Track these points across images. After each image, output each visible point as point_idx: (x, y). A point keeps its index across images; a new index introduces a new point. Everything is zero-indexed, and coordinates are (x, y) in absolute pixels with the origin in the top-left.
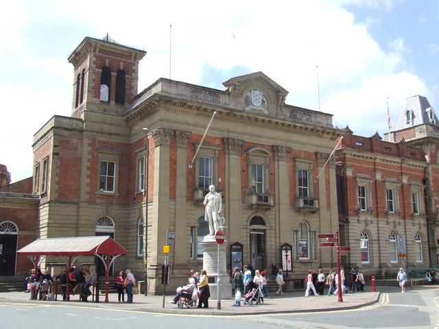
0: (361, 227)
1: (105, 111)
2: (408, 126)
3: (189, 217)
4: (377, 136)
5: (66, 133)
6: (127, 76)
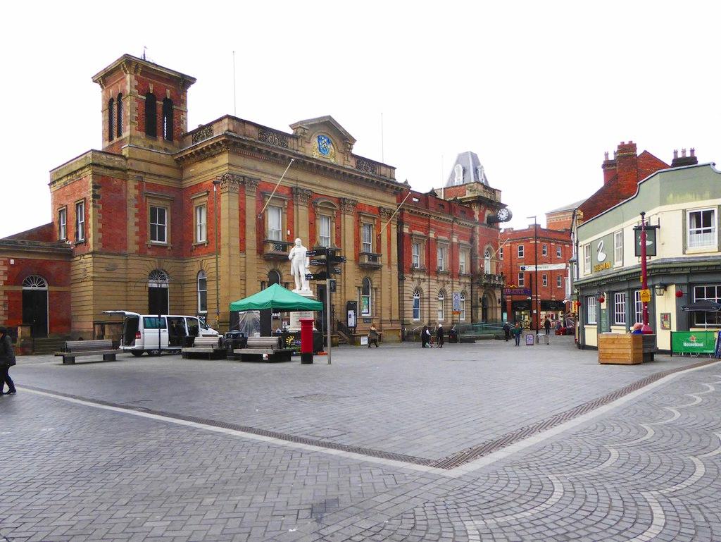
0: (415, 284)
5: (107, 172)
6: (174, 107)
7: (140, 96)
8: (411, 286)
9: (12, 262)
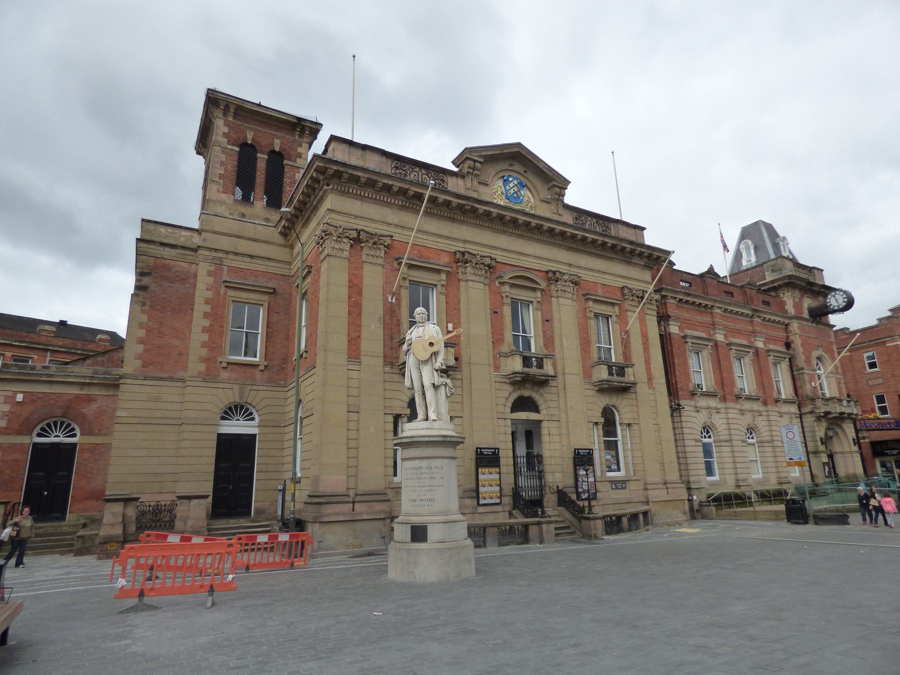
1: (243, 215)
3: (389, 394)
4: (711, 272)
6: (285, 162)
7: (230, 147)
8: (695, 420)
9: (20, 397)
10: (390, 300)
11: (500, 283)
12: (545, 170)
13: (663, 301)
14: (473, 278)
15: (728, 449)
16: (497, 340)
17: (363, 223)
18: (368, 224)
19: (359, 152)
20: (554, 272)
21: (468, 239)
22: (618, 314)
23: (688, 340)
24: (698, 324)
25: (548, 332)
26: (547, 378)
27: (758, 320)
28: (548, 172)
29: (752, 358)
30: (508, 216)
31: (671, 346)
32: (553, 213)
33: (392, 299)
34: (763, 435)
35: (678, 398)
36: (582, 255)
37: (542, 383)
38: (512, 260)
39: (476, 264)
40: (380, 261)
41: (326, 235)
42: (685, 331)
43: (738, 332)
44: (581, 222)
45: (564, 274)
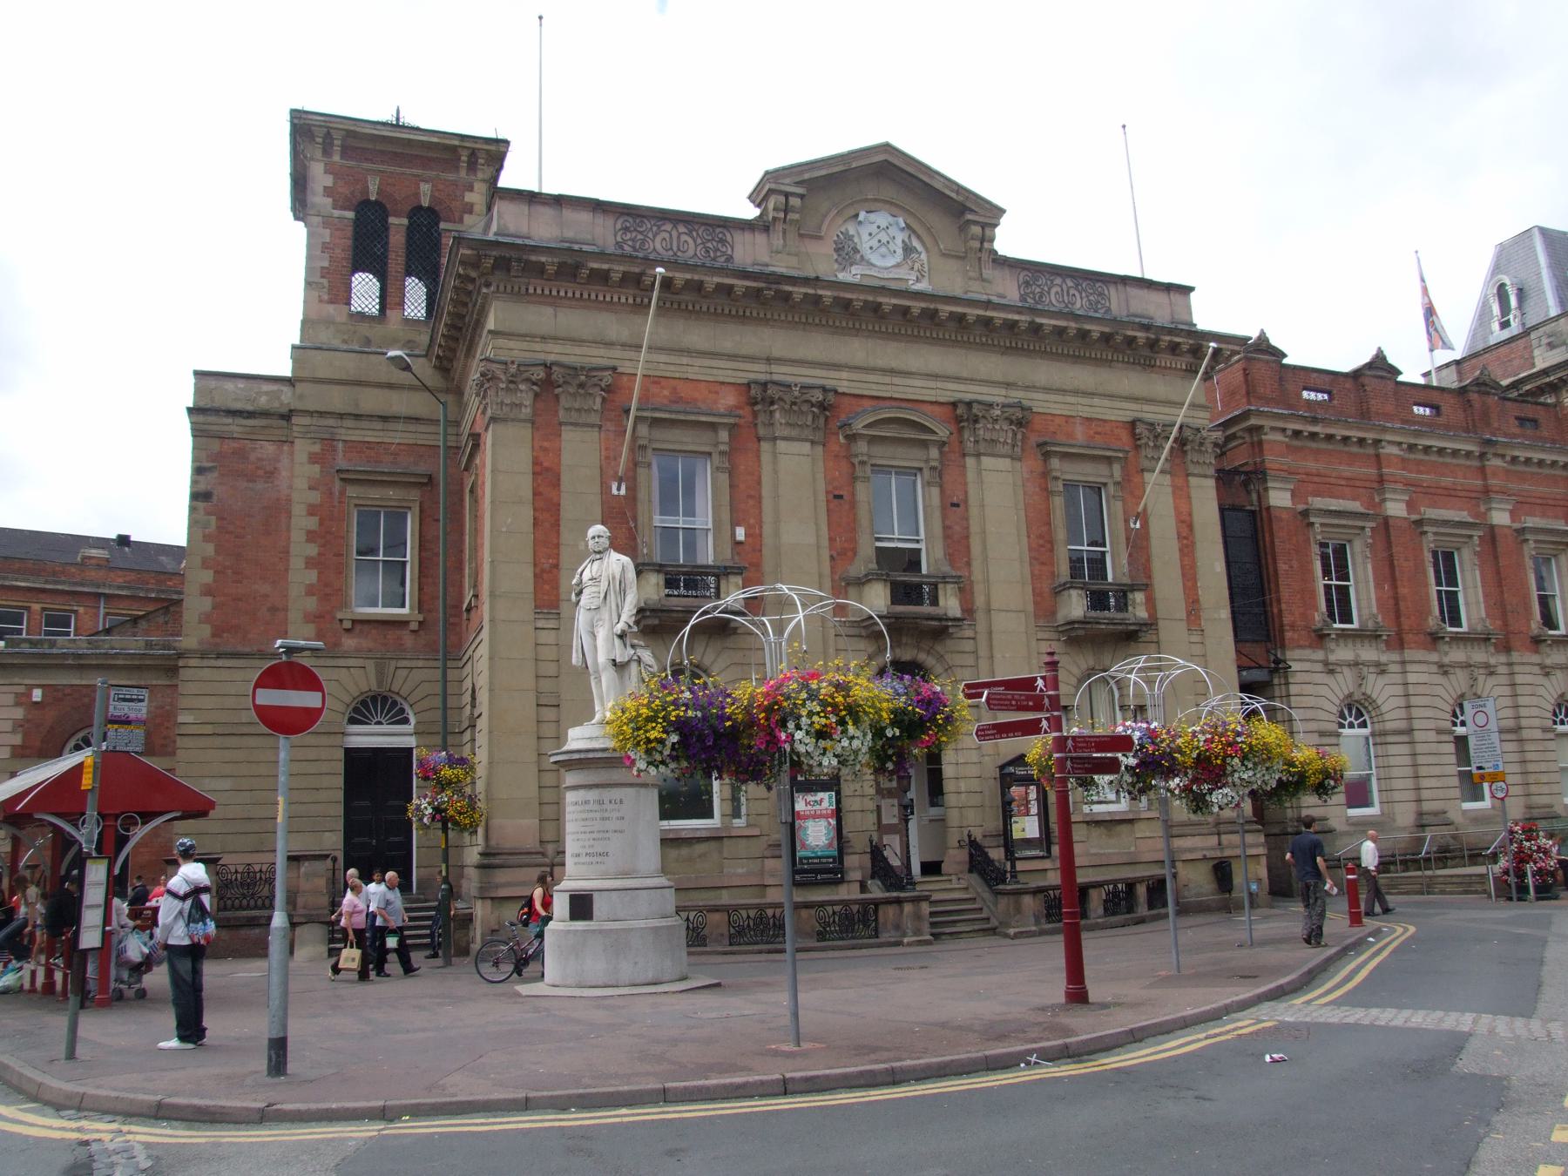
0: (1344, 683)
1: (368, 342)
2: (1506, 334)
4: (1380, 367)
5: (235, 426)
6: (442, 225)
7: (337, 213)
8: (1323, 690)
9: (37, 695)
10: (615, 492)
11: (847, 437)
12: (948, 192)
13: (1255, 439)
14: (786, 432)
15: (1405, 749)
16: (843, 553)
17: (558, 348)
18: (569, 349)
19: (547, 212)
20: (969, 404)
21: (776, 353)
22: (1119, 479)
23: (1312, 519)
24: (1343, 482)
25: (957, 528)
26: (944, 623)
27: (1498, 462)
28: (953, 195)
29: (1478, 549)
30: (858, 300)
31: (1272, 534)
32: (970, 279)
33: (619, 489)
34: (1387, 717)
35: (1283, 646)
36: (1039, 361)
37: (940, 631)
38: (874, 386)
39: (794, 403)
40: (594, 419)
41: (488, 380)
42: (1310, 499)
43: (1445, 492)
44: (1038, 290)
45: (991, 405)
